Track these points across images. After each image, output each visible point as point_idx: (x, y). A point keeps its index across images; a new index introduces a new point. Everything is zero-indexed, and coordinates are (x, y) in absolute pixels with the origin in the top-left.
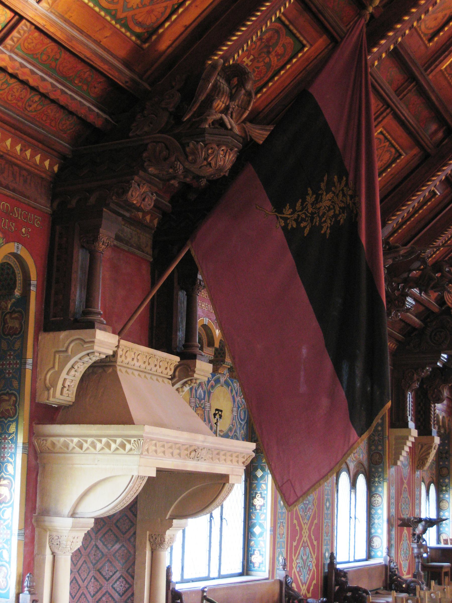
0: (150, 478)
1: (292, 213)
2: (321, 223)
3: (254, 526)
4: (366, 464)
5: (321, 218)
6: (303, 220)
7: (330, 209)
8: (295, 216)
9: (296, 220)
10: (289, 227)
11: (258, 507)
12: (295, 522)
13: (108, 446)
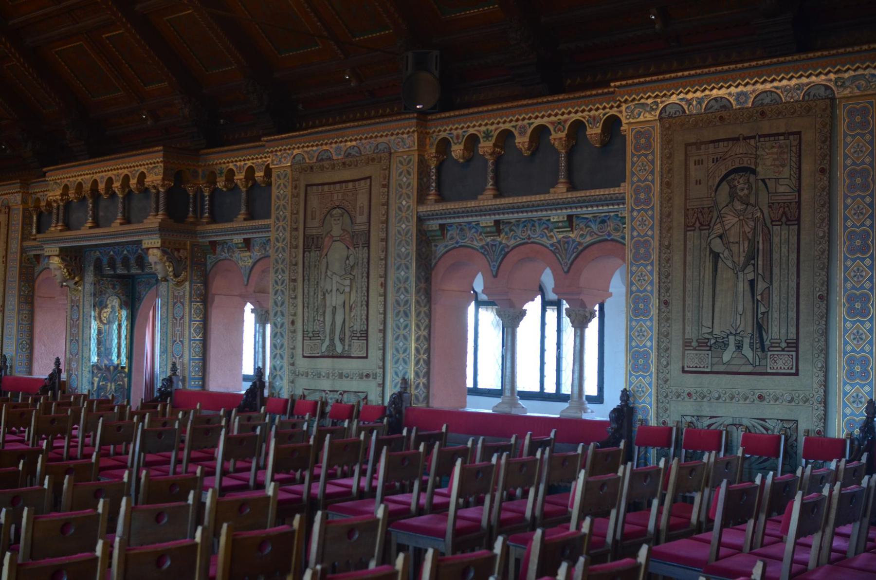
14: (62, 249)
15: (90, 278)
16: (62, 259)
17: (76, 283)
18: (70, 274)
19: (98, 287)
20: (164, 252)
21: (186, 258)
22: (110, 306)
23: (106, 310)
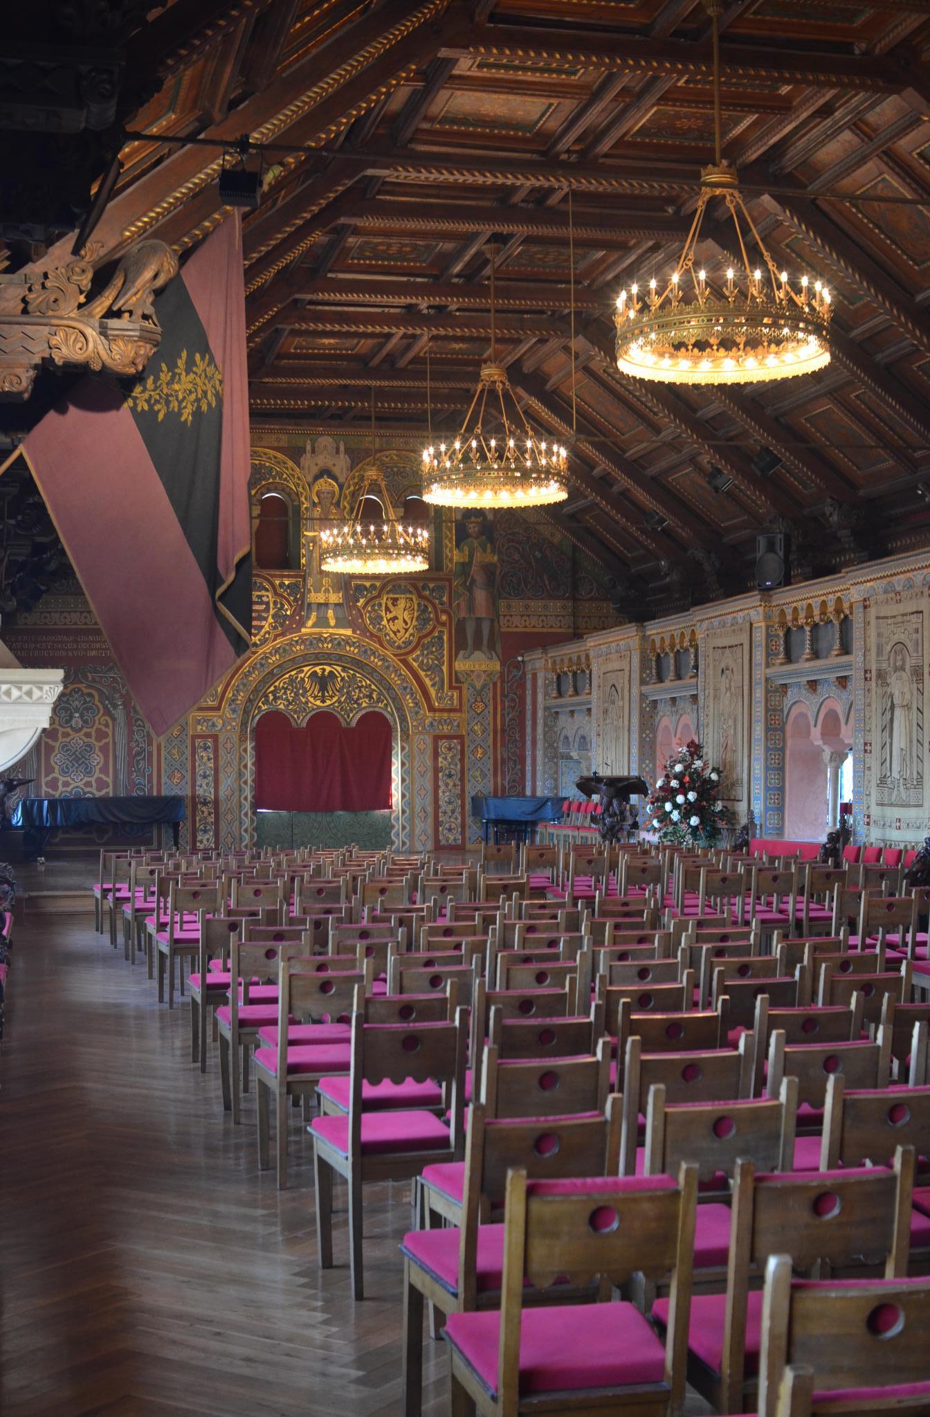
1: (143, 392)
2: (180, 409)
6: (157, 402)
7: (191, 392)
8: (146, 395)
9: (148, 401)
10: (139, 409)
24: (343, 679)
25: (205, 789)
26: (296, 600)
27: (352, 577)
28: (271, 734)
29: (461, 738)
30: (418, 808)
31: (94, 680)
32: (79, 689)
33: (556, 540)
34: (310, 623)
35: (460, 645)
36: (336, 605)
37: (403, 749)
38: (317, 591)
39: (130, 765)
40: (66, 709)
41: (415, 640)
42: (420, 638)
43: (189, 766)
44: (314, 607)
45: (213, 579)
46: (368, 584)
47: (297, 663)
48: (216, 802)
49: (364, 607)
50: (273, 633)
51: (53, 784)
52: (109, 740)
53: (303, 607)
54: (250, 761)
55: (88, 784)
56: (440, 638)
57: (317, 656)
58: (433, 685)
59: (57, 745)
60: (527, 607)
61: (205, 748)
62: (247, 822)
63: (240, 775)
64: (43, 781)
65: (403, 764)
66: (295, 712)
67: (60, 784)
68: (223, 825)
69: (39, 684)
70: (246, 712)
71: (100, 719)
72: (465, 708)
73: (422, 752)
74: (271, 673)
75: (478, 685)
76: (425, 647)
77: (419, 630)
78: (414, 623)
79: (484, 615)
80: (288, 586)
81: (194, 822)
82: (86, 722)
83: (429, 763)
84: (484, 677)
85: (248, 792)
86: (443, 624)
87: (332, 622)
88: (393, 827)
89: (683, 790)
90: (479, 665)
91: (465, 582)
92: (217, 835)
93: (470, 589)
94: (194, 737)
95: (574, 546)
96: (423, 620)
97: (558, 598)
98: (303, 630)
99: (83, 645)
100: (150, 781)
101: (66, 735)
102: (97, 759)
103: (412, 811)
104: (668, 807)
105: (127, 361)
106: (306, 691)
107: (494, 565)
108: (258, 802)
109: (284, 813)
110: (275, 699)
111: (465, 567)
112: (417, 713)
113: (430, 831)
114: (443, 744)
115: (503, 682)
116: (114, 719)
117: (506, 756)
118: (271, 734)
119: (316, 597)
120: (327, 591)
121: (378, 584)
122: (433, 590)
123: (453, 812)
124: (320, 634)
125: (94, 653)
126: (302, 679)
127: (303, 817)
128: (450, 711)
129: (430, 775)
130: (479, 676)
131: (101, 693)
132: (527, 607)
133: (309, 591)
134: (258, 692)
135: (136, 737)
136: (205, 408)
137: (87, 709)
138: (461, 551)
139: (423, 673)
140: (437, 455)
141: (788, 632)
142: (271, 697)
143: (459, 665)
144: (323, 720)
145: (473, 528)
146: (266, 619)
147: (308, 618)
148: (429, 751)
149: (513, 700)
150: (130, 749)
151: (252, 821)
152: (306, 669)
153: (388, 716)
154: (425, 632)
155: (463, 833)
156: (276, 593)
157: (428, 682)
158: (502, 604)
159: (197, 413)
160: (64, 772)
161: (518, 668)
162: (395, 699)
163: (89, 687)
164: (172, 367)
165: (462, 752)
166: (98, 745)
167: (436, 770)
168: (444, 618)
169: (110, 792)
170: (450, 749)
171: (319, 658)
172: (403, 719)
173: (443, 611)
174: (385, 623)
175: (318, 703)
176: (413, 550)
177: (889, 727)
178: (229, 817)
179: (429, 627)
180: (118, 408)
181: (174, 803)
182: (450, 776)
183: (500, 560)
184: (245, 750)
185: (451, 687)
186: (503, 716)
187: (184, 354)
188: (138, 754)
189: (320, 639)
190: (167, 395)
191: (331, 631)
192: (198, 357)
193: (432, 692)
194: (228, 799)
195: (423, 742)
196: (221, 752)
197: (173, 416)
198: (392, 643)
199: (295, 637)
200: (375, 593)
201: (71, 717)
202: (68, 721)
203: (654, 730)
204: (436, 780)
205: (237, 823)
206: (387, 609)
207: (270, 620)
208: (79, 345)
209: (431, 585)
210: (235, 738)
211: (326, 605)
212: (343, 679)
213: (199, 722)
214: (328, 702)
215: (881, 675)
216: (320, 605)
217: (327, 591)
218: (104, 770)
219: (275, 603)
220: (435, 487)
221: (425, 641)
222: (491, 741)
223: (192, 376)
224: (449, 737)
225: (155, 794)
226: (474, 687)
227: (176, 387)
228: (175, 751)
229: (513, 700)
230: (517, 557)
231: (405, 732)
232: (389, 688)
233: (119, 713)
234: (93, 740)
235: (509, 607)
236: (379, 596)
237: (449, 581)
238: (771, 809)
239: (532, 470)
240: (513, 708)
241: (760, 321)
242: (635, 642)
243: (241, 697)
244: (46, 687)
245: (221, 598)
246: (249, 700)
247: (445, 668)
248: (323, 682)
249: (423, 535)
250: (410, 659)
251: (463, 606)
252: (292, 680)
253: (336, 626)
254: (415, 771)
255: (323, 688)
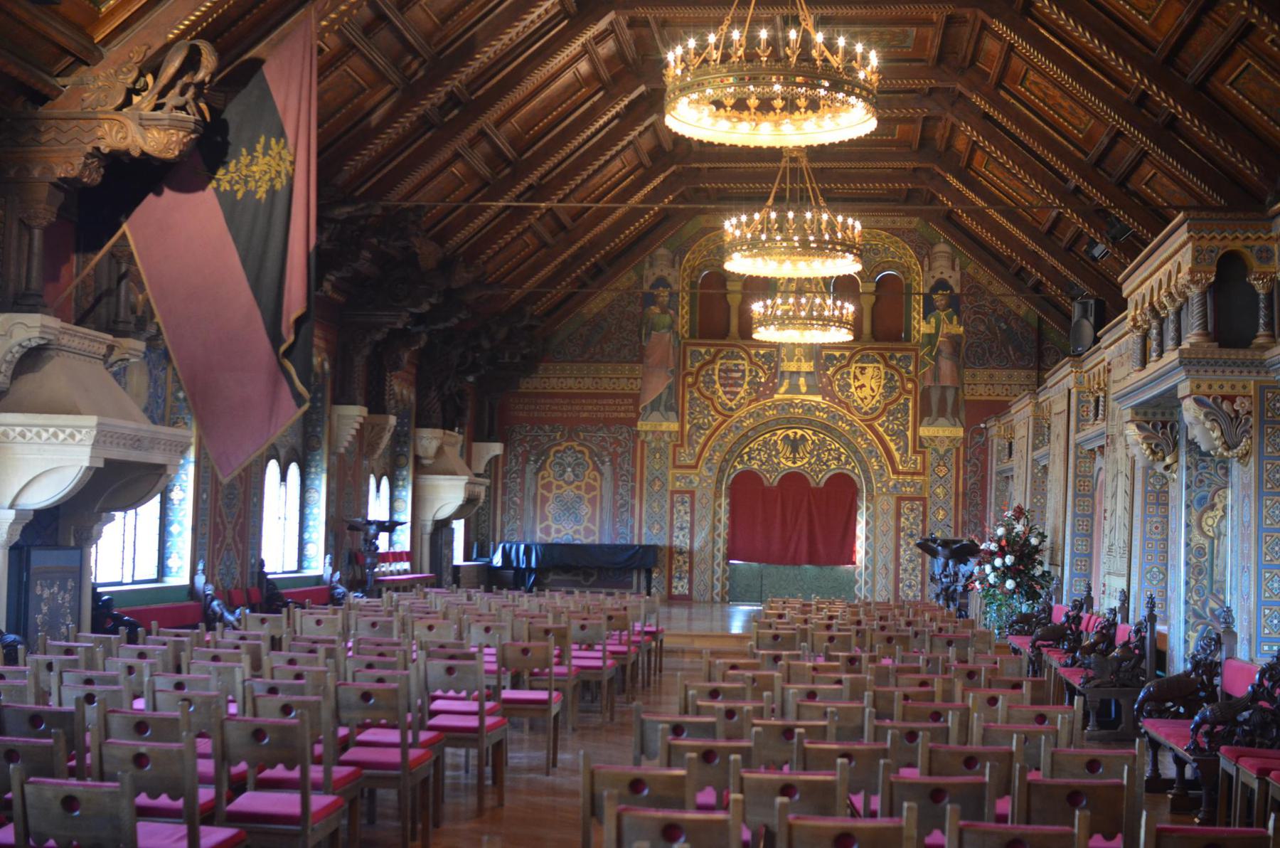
0: (98, 469)
3: (171, 523)
4: (300, 449)
5: (257, 182)
6: (237, 182)
8: (228, 177)
9: (229, 182)
11: (176, 502)
12: (218, 520)
13: (55, 435)
14: (1137, 409)
15: (1183, 460)
16: (1138, 427)
17: (1167, 468)
18: (1154, 453)
19: (1195, 473)
20: (1198, 402)
21: (1249, 413)
22: (1219, 506)
23: (1211, 514)
24: (813, 442)
25: (681, 540)
26: (770, 368)
27: (823, 346)
28: (745, 491)
29: (923, 500)
30: (880, 565)
31: (585, 439)
32: (572, 447)
33: (1022, 312)
34: (782, 390)
35: (925, 412)
36: (807, 373)
37: (868, 508)
38: (790, 360)
39: (614, 516)
40: (560, 464)
41: (882, 406)
42: (886, 405)
43: (668, 518)
44: (787, 375)
45: (276, 339)
46: (837, 354)
47: (771, 426)
48: (691, 553)
49: (834, 375)
50: (748, 399)
51: (547, 531)
52: (597, 493)
53: (776, 375)
54: (724, 516)
55: (577, 532)
56: (906, 405)
57: (789, 420)
58: (898, 450)
59: (551, 496)
60: (991, 376)
61: (683, 503)
62: (719, 572)
63: (714, 528)
64: (538, 527)
65: (867, 523)
66: (768, 471)
67: (553, 530)
68: (696, 572)
69: (78, 428)
70: (721, 471)
71: (590, 473)
72: (928, 471)
73: (885, 513)
74: (745, 435)
75: (942, 451)
76: (891, 413)
77: (885, 397)
78: (881, 390)
79: (948, 384)
80: (763, 356)
81: (670, 569)
82: (576, 476)
83: (892, 523)
84: (947, 442)
85: (721, 545)
86: (909, 392)
87: (804, 389)
88: (856, 582)
89: (1002, 553)
90: (943, 432)
91: (931, 351)
92: (690, 582)
93: (936, 359)
94: (673, 493)
95: (1039, 318)
96: (889, 389)
97: (1023, 368)
98: (776, 396)
99: (577, 408)
100: (632, 532)
101: (559, 487)
102: (585, 510)
103: (874, 568)
104: (988, 568)
105: (162, 147)
106: (778, 453)
107: (959, 336)
108: (730, 555)
109: (755, 565)
110: (750, 459)
111: (931, 338)
112: (881, 475)
113: (891, 587)
114: (906, 506)
115: (966, 447)
116: (601, 474)
117: (966, 518)
118: (745, 491)
119: (792, 367)
120: (799, 360)
121: (847, 354)
122: (900, 360)
123: (914, 570)
124: (791, 400)
125: (585, 415)
126: (776, 442)
127: (772, 569)
128: (913, 474)
129: (892, 533)
130: (942, 442)
131: (591, 451)
132: (991, 376)
133: (783, 360)
134: (734, 452)
135: (621, 491)
136: (278, 186)
137: (578, 465)
138: (928, 323)
139: (888, 438)
140: (739, 225)
141: (1097, 401)
142: (746, 458)
143: (924, 431)
144: (794, 479)
145: (939, 298)
146: (741, 386)
147: (781, 385)
148: (892, 512)
149: (975, 465)
150: (615, 502)
151: (724, 571)
152: (779, 432)
153: (855, 478)
154: (891, 399)
155: (922, 591)
156: (751, 362)
157: (893, 446)
158: (967, 373)
159: (272, 192)
160: (556, 520)
161: (981, 434)
162: (861, 462)
163: (580, 445)
164: (252, 150)
165: (924, 514)
166: (587, 496)
167: (898, 530)
168: (910, 386)
169: (594, 539)
170: (912, 510)
171: (791, 422)
172: (868, 481)
173: (909, 380)
174: (853, 390)
175: (790, 464)
176: (841, 322)
177: (1114, 495)
178: (703, 566)
179: (895, 395)
180: (202, 187)
181: (652, 550)
182: (911, 536)
183: (966, 331)
184: (720, 506)
185: (915, 452)
186: (965, 480)
187: (262, 140)
188: (622, 506)
189: (791, 404)
190: (246, 176)
191: (802, 397)
192: (273, 141)
193: (897, 456)
194: (702, 549)
195: (886, 503)
196: (697, 506)
197: (249, 194)
198: (859, 409)
199: (768, 402)
200: (844, 362)
201: (564, 472)
202: (561, 475)
203: (1044, 496)
204: (898, 537)
205: (709, 572)
206: (855, 377)
207: (746, 386)
208: (120, 135)
209: (898, 355)
210: (710, 494)
211: (798, 373)
212: (813, 442)
213: (677, 479)
214: (799, 464)
215: (1113, 442)
216: (792, 373)
217: (799, 360)
218: (592, 520)
219: (751, 371)
220: (736, 256)
221: (891, 407)
222: (952, 503)
223: (268, 158)
224: (912, 499)
225: (636, 542)
226: (936, 451)
227: (254, 168)
228: (655, 505)
229: (975, 465)
230: (982, 328)
231: (870, 492)
232: (856, 452)
233: (607, 469)
234: (582, 493)
235: (974, 376)
236: (848, 365)
237: (916, 350)
238: (1076, 575)
239: (829, 242)
240: (975, 473)
241: (818, 80)
242: (1029, 409)
243: (717, 457)
244: (84, 431)
245: (287, 354)
246: (725, 461)
247: (909, 433)
248: (795, 445)
249: (850, 308)
250: (876, 424)
251: (929, 376)
252: (766, 443)
253: (807, 393)
254: (878, 530)
255: (795, 450)
